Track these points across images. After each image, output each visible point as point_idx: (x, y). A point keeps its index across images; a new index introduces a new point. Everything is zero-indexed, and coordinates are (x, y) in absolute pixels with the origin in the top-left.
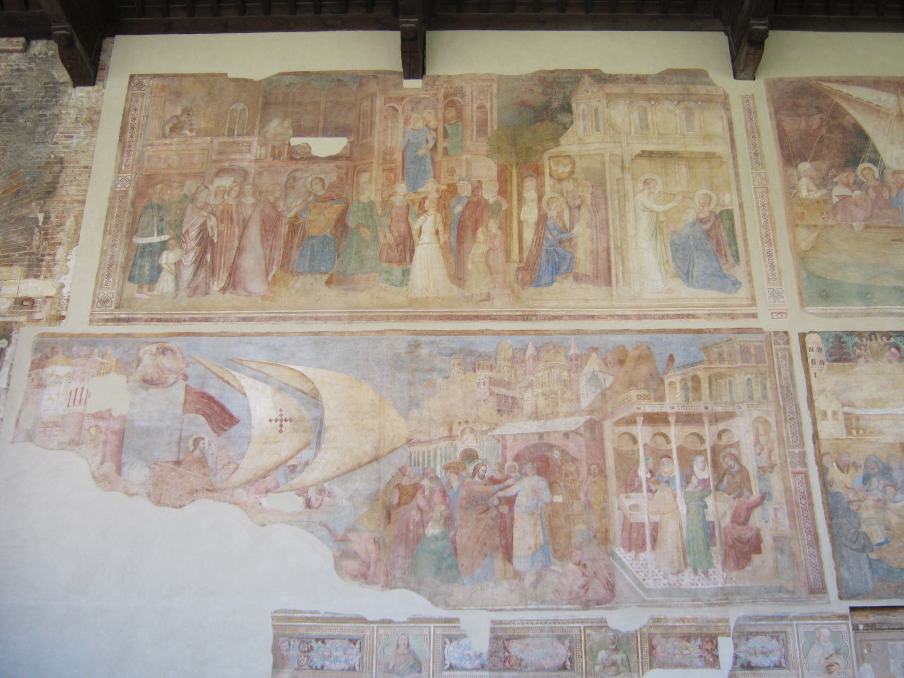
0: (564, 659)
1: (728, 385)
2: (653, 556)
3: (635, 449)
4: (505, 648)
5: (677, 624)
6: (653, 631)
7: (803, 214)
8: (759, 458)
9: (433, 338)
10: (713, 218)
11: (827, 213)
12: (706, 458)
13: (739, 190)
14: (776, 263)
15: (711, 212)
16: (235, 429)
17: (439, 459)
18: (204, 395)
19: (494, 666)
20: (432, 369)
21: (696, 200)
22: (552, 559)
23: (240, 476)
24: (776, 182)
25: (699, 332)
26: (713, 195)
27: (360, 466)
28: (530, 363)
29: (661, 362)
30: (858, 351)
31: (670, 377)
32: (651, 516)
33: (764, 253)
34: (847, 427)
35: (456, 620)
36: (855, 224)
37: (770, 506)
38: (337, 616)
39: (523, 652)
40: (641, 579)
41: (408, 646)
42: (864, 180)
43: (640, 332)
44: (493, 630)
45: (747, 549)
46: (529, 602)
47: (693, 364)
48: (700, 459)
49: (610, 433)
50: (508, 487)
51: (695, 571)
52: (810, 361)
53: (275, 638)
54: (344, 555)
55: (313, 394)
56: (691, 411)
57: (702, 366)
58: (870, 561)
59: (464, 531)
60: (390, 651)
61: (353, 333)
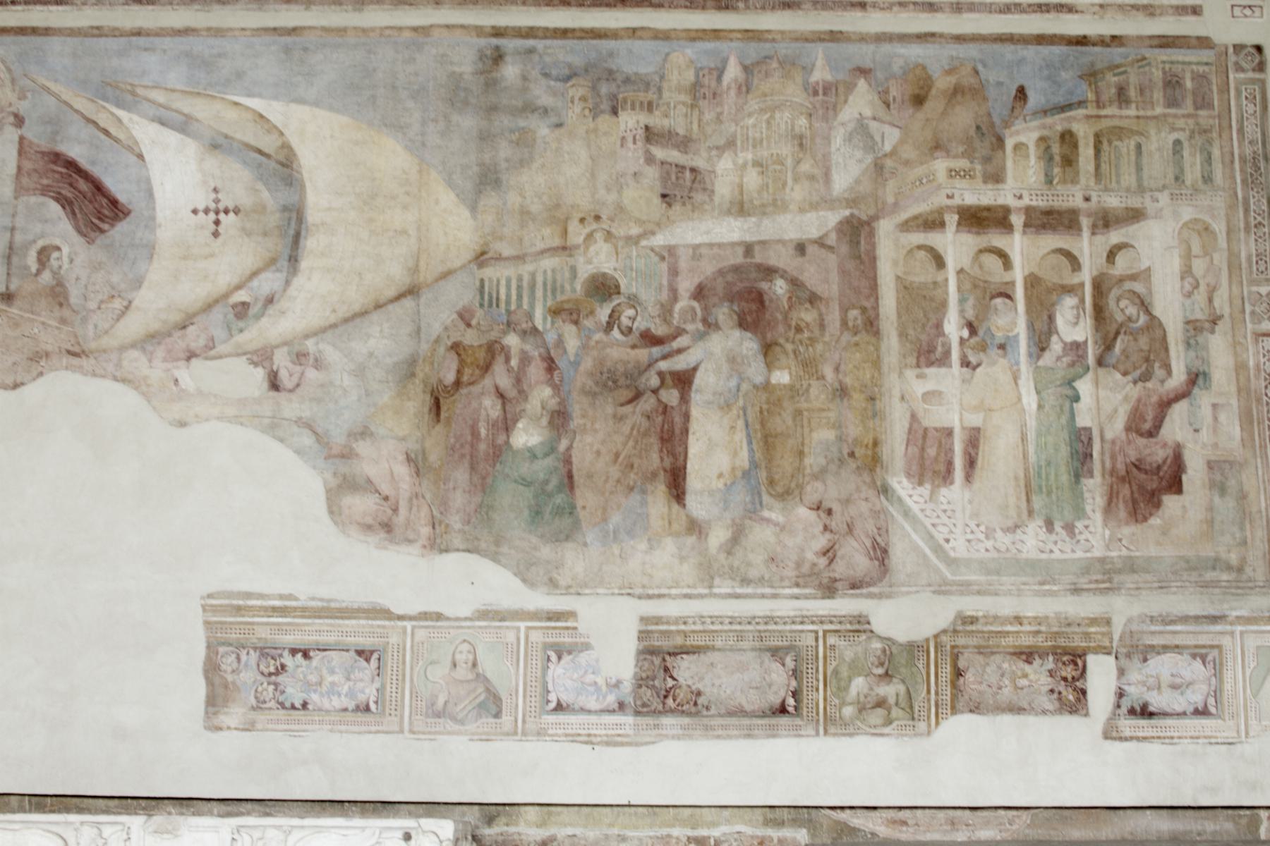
0: (782, 693)
1: (1133, 153)
2: (967, 495)
3: (940, 279)
4: (666, 670)
5: (1009, 628)
6: (961, 641)
8: (1188, 302)
9: (531, 43)
12: (1082, 301)
16: (122, 227)
17: (539, 293)
18: (56, 157)
19: (644, 705)
20: (529, 108)
22: (766, 498)
23: (133, 326)
25: (1082, 41)
27: (378, 306)
28: (731, 98)
29: (1000, 101)
31: (1018, 133)
32: (966, 415)
35: (571, 615)
37: (1204, 400)
38: (333, 605)
39: (701, 679)
40: (940, 538)
41: (475, 665)
43: (960, 39)
44: (643, 635)
45: (1153, 484)
46: (717, 581)
47: (1063, 108)
48: (1070, 301)
49: (891, 248)
50: (680, 351)
51: (1049, 525)
53: (208, 647)
54: (345, 485)
55: (281, 158)
56: (1058, 204)
57: (1081, 112)
59: (589, 439)
60: (439, 673)
61: (364, 31)
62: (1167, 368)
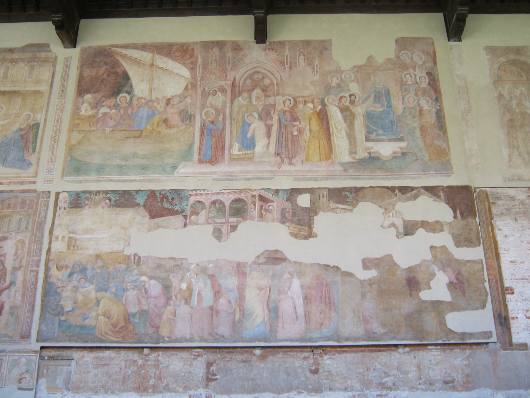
7: (79, 124)
10: (28, 128)
11: (93, 123)
13: (47, 111)
14: (55, 153)
15: (28, 125)
21: (22, 118)
24: (69, 106)
26: (32, 115)
30: (87, 202)
33: (50, 147)
34: (68, 245)
36: (107, 129)
37: (13, 289)
42: (120, 103)
52: (58, 208)
58: (60, 321)
62: (5, 281)
